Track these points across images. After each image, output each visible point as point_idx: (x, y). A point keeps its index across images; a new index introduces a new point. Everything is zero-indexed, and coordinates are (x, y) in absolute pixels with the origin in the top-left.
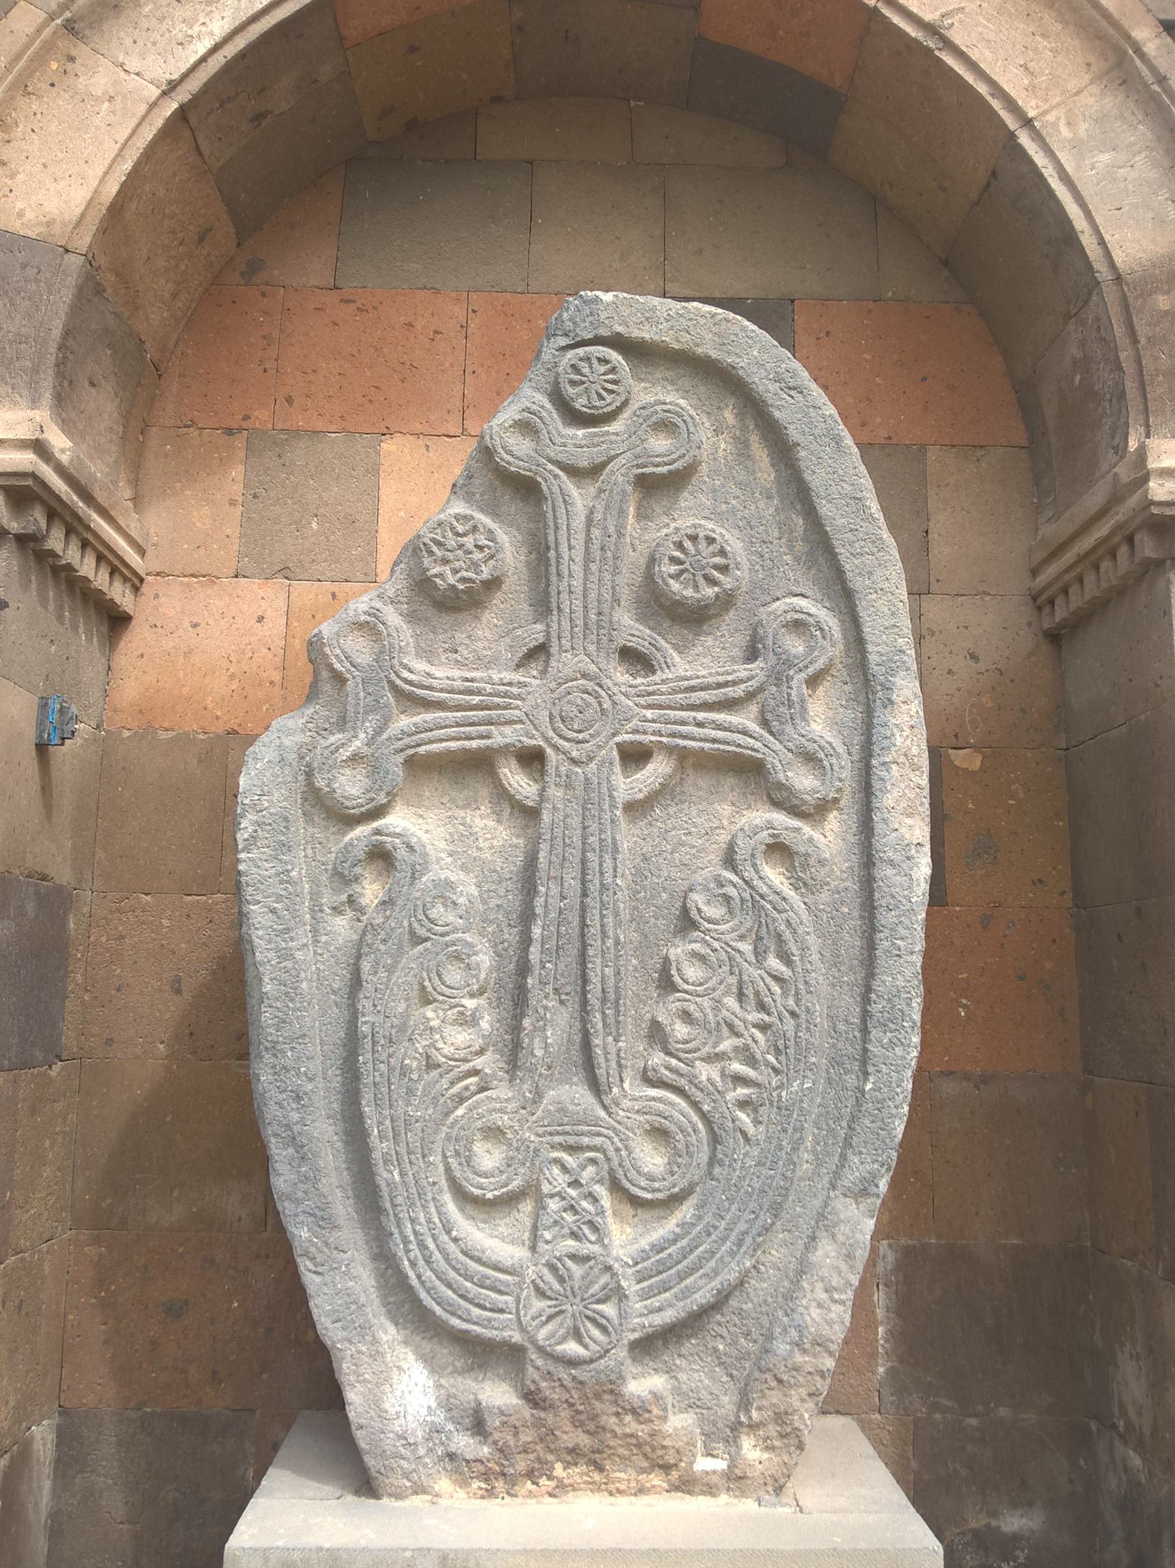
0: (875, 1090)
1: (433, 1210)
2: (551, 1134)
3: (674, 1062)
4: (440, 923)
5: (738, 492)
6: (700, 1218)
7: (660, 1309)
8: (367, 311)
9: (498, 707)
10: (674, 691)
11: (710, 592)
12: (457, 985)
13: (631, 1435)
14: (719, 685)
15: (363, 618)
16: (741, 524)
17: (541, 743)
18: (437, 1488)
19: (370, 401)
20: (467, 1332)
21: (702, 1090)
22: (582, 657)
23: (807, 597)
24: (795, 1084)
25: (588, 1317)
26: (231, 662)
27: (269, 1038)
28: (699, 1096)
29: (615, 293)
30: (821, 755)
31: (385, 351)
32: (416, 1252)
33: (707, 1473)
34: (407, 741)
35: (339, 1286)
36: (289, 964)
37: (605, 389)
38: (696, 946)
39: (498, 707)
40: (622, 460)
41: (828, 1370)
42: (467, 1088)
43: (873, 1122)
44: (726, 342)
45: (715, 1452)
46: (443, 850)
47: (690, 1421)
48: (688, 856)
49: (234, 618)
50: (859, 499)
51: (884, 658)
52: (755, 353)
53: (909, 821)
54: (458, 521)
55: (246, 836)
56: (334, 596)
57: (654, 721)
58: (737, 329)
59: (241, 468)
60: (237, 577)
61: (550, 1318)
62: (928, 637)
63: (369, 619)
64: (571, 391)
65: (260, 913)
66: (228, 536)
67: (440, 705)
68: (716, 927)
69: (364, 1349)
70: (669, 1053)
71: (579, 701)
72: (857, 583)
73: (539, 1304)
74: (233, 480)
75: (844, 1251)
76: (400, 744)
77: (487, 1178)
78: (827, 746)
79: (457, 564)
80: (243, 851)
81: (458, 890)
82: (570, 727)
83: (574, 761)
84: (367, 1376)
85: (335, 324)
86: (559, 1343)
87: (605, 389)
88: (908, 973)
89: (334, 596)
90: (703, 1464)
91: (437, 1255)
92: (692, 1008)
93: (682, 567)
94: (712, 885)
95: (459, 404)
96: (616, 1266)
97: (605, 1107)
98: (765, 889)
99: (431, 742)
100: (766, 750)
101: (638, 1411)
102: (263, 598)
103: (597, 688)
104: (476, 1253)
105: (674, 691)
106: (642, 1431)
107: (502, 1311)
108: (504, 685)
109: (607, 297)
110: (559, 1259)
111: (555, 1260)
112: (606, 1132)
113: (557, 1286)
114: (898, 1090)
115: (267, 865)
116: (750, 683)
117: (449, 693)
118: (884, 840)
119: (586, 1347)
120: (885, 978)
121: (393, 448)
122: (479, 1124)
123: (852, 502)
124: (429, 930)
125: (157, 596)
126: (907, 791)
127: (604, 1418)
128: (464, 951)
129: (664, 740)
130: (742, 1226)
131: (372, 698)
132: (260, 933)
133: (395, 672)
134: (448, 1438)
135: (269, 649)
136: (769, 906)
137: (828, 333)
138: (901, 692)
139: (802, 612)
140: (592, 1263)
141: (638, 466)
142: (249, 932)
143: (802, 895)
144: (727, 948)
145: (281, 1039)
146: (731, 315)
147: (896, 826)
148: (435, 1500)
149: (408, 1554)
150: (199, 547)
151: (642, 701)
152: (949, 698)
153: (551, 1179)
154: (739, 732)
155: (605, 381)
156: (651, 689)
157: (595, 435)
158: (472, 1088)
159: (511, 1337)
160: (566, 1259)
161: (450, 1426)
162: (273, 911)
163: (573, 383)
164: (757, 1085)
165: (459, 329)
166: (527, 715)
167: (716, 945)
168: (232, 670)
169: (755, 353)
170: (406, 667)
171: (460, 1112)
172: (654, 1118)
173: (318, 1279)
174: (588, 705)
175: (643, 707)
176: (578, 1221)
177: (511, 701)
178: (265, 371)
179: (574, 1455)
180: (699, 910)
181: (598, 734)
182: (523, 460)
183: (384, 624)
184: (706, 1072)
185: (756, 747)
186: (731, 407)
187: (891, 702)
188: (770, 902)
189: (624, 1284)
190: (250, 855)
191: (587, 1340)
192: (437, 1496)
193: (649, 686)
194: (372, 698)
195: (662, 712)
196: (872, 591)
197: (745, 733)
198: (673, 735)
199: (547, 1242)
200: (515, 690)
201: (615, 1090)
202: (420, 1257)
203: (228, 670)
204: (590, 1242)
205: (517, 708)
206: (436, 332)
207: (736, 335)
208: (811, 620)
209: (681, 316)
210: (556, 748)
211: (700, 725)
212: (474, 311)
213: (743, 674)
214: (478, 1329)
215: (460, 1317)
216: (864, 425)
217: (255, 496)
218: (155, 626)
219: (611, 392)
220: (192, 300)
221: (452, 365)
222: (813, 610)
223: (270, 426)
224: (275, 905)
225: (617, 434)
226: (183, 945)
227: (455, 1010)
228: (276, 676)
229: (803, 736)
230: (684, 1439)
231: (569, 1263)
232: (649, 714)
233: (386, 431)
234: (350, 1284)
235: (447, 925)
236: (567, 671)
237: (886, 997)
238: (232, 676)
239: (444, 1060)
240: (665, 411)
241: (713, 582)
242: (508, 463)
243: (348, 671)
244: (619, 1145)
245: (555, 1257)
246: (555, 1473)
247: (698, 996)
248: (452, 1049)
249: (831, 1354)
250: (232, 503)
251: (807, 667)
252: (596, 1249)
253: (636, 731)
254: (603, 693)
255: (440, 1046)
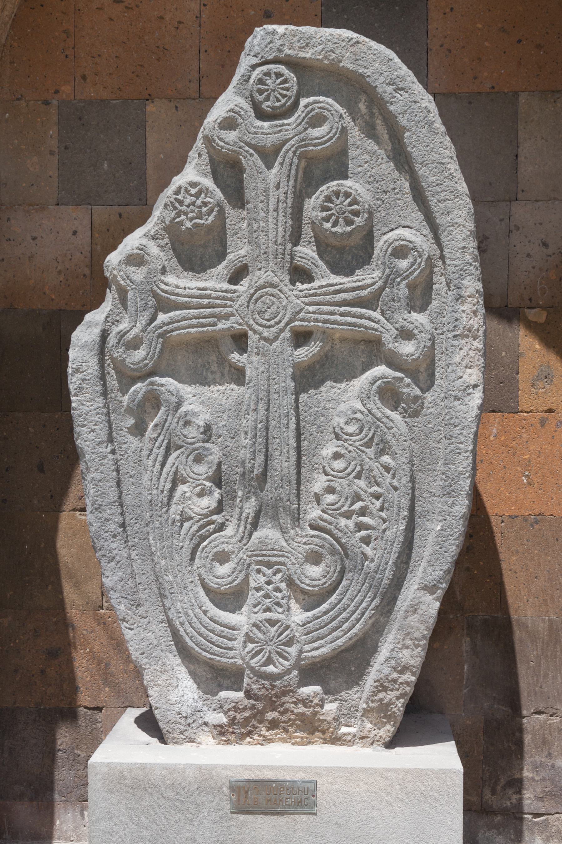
0: (442, 530)
1: (191, 595)
2: (257, 556)
3: (325, 516)
4: (190, 436)
5: (368, 158)
6: (340, 601)
7: (317, 648)
8: (132, 8)
9: (218, 306)
10: (325, 294)
11: (348, 229)
12: (200, 473)
13: (303, 714)
14: (354, 289)
15: (136, 251)
16: (370, 180)
17: (246, 327)
18: (199, 740)
19: (137, 76)
20: (212, 659)
21: (341, 531)
22: (270, 273)
23: (411, 228)
24: (395, 527)
25: (277, 652)
26: (58, 262)
27: (97, 503)
28: (340, 534)
29: (286, 26)
30: (416, 331)
31: (146, 38)
32: (183, 618)
33: (345, 734)
34: (165, 328)
35: (142, 635)
36: (105, 461)
37: (281, 94)
38: (338, 449)
39: (218, 306)
40: (292, 142)
41: (412, 682)
42: (208, 531)
43: (441, 548)
44: (358, 58)
45: (349, 724)
46: (189, 393)
47: (336, 707)
48: (336, 394)
49: (58, 233)
50: (443, 164)
51: (457, 268)
52: (377, 65)
53: (469, 371)
54: (191, 186)
55: (75, 387)
56: (120, 215)
57: (314, 313)
58: (364, 49)
59: (55, 128)
60: (58, 205)
61: (258, 653)
62: (514, 231)
63: (140, 252)
64: (260, 98)
65: (87, 432)
66: (50, 177)
67: (186, 306)
68: (351, 438)
69: (157, 668)
70: (323, 511)
71: (268, 301)
72: (441, 220)
73: (250, 646)
74: (51, 137)
75: (422, 619)
76: (160, 331)
77: (221, 579)
78: (420, 325)
79: (190, 215)
80: (74, 396)
81: (200, 417)
82: (263, 317)
83: (265, 339)
84: (159, 682)
85: (111, 19)
86: (261, 666)
87: (281, 94)
88: (465, 463)
89: (120, 215)
90: (344, 730)
91: (194, 620)
92: (337, 484)
93: (330, 212)
94: (349, 412)
95: (196, 75)
96: (293, 625)
97: (286, 541)
98: (379, 415)
99: (179, 329)
100: (381, 329)
101: (305, 702)
102: (76, 219)
103: (278, 292)
104: (216, 618)
105: (325, 294)
106: (308, 711)
107: (231, 649)
108: (222, 292)
109: (281, 29)
110: (261, 622)
111: (259, 622)
112: (286, 554)
113: (260, 636)
114: (456, 530)
115: (88, 404)
116: (373, 287)
117: (189, 298)
118: (453, 384)
119: (276, 667)
120: (451, 466)
121: (154, 109)
122: (215, 550)
123: (439, 165)
124: (183, 441)
125: (9, 219)
126: (470, 352)
127: (288, 704)
128: (204, 453)
129: (320, 324)
130: (364, 605)
131: (144, 302)
132: (88, 443)
133: (157, 285)
134: (204, 715)
135: (82, 253)
136: (382, 425)
137: (452, 9)
138: (468, 289)
139: (406, 240)
140: (279, 624)
141: (302, 146)
142: (82, 442)
143: (404, 417)
144: (357, 450)
145: (103, 503)
146: (362, 38)
147: (461, 374)
148: (198, 745)
149: (182, 766)
150: (32, 185)
151: (306, 300)
152: (526, 274)
153: (256, 580)
154: (366, 319)
155: (281, 88)
156: (311, 292)
157: (276, 126)
158: (211, 530)
159: (236, 662)
160: (265, 622)
161: (205, 708)
162: (93, 431)
163: (261, 92)
164: (374, 528)
165: (195, 19)
166: (237, 310)
167: (351, 448)
168: (59, 268)
169: (377, 65)
170: (163, 282)
171: (205, 544)
172: (314, 546)
173: (131, 632)
174: (273, 303)
175: (307, 304)
176: (271, 602)
177: (226, 302)
178: (67, 56)
179: (273, 725)
180: (341, 429)
181: (280, 322)
182: (229, 144)
183: (148, 255)
184: (343, 522)
185: (376, 327)
186: (363, 100)
187: (461, 296)
188: (383, 423)
189: (297, 635)
190: (78, 398)
191: (277, 664)
192: (199, 743)
193: (310, 290)
194: (144, 302)
195: (319, 307)
196: (450, 224)
197: (370, 319)
198: (325, 322)
199: (255, 613)
200: (229, 295)
201: (292, 531)
202: (185, 620)
203: (57, 267)
204: (279, 613)
205: (231, 306)
206: (180, 22)
207: (365, 53)
208: (411, 245)
209: (329, 41)
210: (255, 332)
211: (342, 314)
212: (205, 5)
213: (369, 281)
214: (218, 658)
215: (208, 652)
216: (475, 78)
217: (66, 148)
218: (10, 240)
219: (284, 96)
220: (14, 8)
221: (191, 46)
222: (413, 239)
223: (72, 97)
224: (95, 427)
225: (288, 125)
226: (43, 444)
227: (200, 487)
228: (87, 271)
229: (405, 320)
230: (333, 716)
231: (267, 625)
232: (311, 309)
233: (148, 97)
234: (149, 634)
235: (194, 438)
236: (261, 282)
237: (451, 477)
238: (60, 272)
239: (195, 515)
240: (319, 108)
241: (349, 222)
242: (222, 148)
243: (129, 285)
244: (294, 561)
245: (259, 621)
246: (262, 733)
247: (340, 478)
248: (199, 509)
249: (413, 674)
250: (52, 153)
251: (408, 276)
252: (282, 616)
253: (303, 320)
254: (282, 296)
255: (192, 507)
